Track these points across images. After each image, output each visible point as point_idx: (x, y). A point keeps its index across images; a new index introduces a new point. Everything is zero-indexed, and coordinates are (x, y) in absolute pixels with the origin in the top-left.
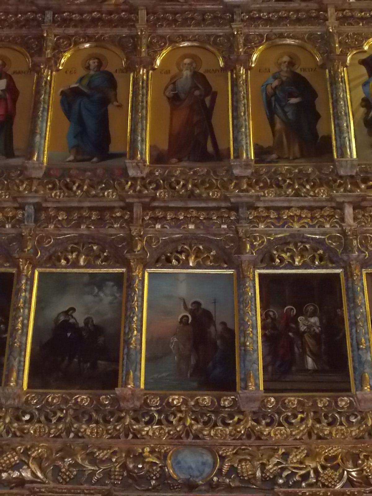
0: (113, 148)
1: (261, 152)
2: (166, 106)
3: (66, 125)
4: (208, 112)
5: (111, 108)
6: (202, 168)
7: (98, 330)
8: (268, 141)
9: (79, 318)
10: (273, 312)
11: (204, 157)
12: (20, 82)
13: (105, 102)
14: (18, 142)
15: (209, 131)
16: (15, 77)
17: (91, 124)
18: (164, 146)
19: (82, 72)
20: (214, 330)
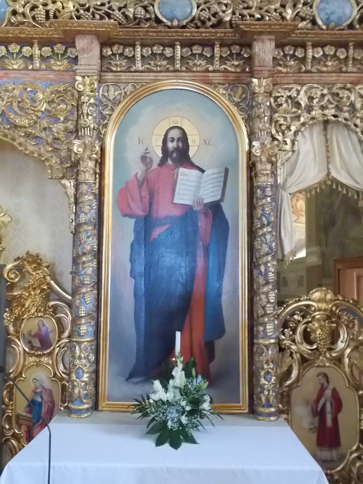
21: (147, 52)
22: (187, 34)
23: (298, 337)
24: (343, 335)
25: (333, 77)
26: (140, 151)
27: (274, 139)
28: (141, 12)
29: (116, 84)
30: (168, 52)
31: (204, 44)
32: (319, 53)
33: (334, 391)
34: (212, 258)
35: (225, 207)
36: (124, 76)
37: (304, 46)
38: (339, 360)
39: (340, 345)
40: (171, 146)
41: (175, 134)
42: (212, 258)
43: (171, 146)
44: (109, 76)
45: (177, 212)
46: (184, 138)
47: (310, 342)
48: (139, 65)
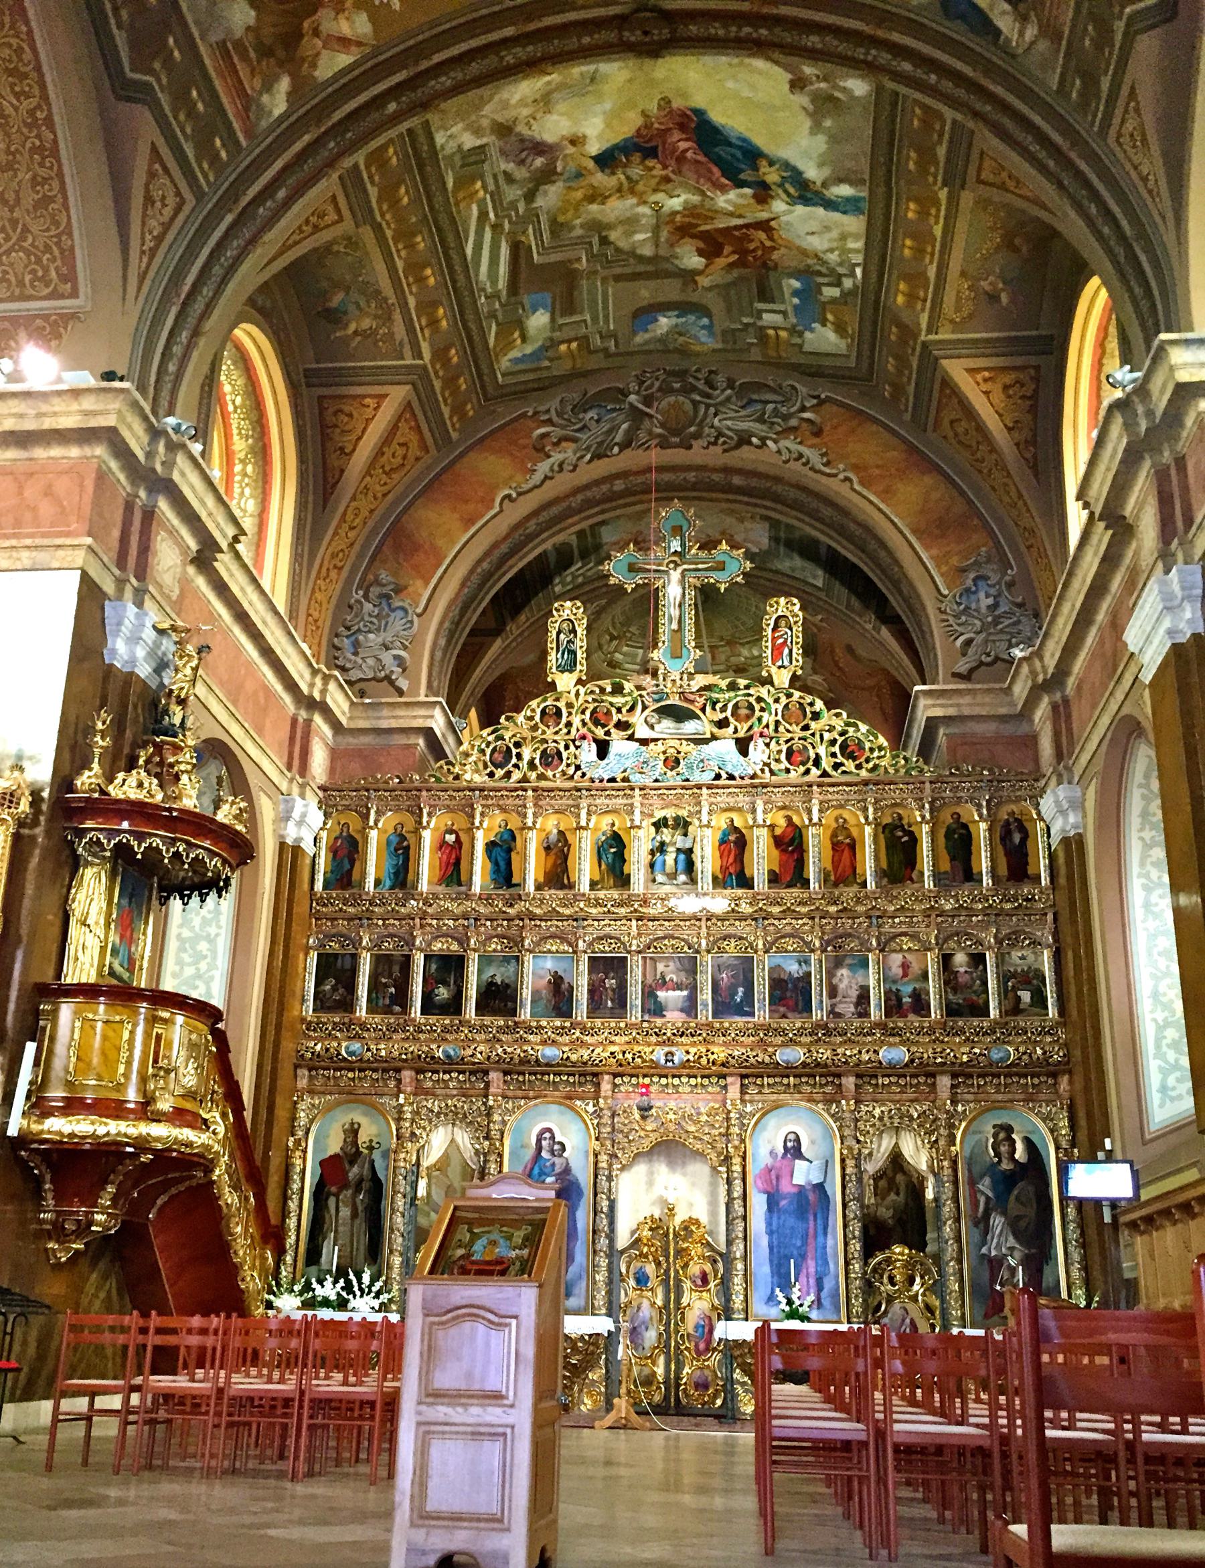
0: (514, 881)
1: (593, 885)
2: (543, 853)
3: (489, 865)
4: (566, 858)
5: (513, 855)
6: (561, 893)
7: (508, 986)
8: (597, 878)
9: (498, 980)
10: (594, 977)
11: (562, 887)
12: (463, 837)
13: (509, 850)
14: (464, 878)
15: (566, 870)
16: (461, 834)
17: (502, 864)
18: (541, 880)
19: (497, 830)
20: (565, 986)
21: (771, 1081)
22: (797, 1071)
23: (885, 1280)
24: (918, 1280)
25: (898, 1097)
26: (769, 1148)
27: (859, 1142)
28: (767, 1060)
29: (751, 1102)
30: (785, 1081)
31: (809, 1076)
32: (886, 1081)
33: (912, 1321)
34: (819, 1221)
35: (827, 1186)
36: (757, 1097)
37: (876, 1077)
38: (914, 1298)
39: (916, 1287)
40: (789, 1144)
41: (792, 1137)
42: (819, 1221)
43: (789, 1144)
44: (747, 1097)
45: (795, 1190)
46: (798, 1140)
47: (893, 1284)
48: (766, 1090)
